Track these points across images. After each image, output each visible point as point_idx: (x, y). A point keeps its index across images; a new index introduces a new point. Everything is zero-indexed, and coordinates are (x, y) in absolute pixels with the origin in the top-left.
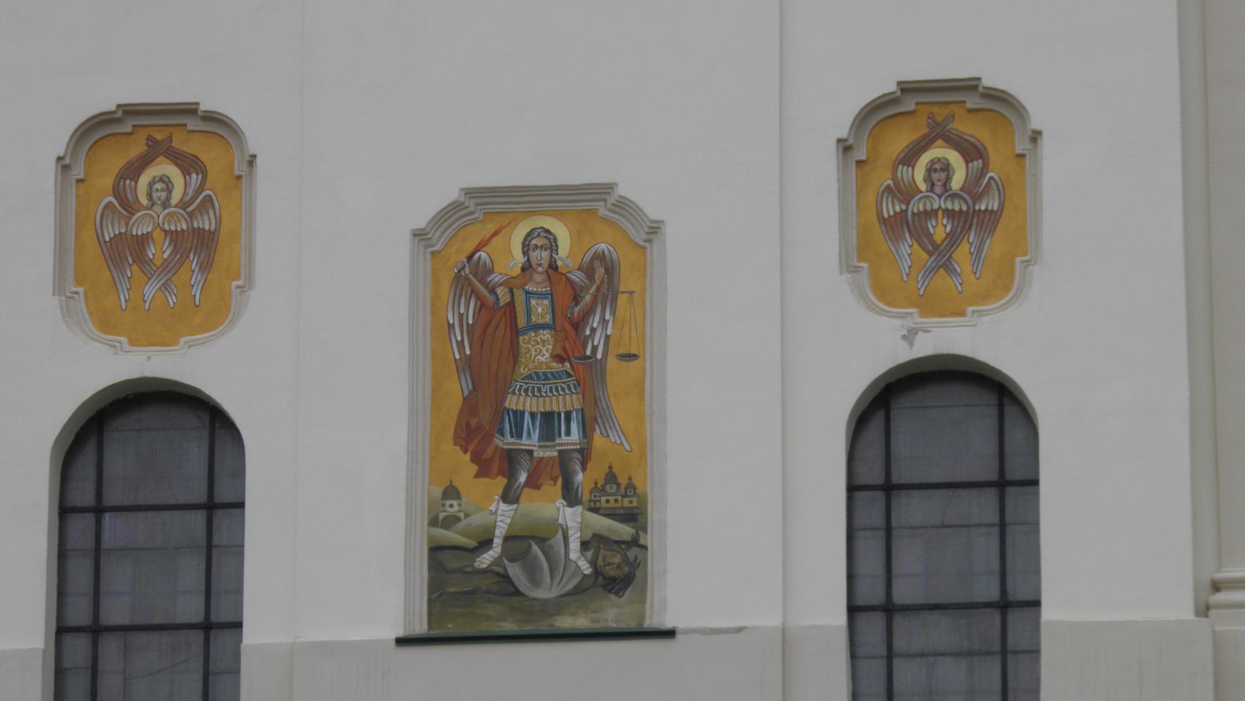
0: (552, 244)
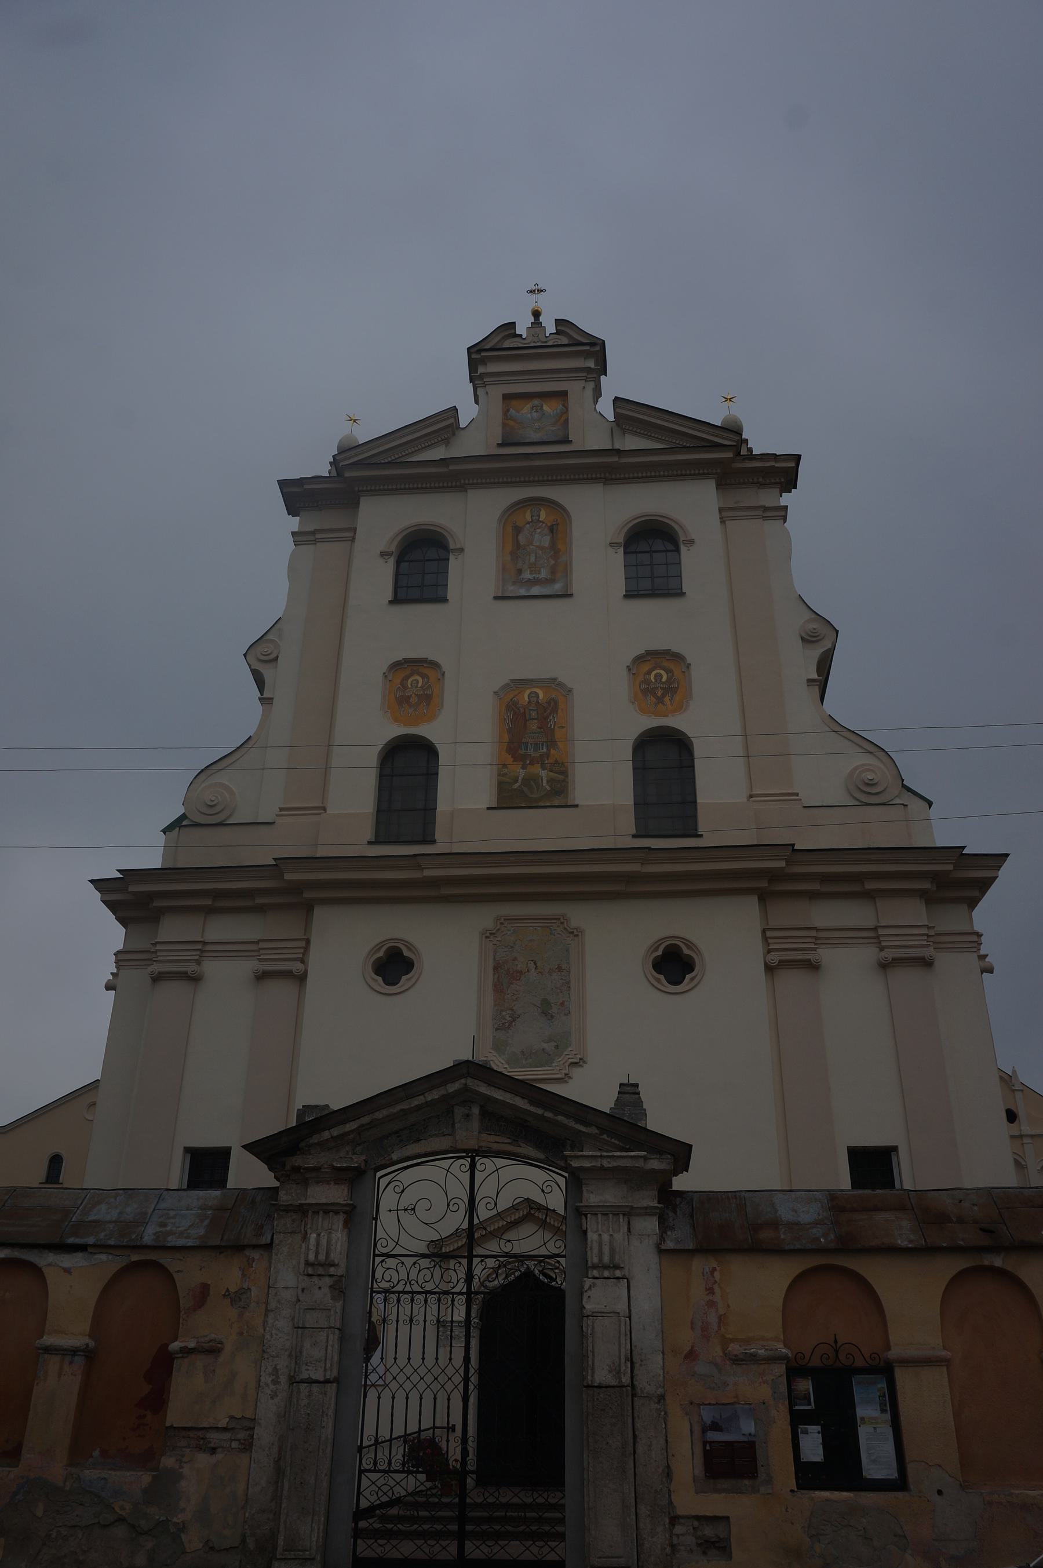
0: (537, 695)
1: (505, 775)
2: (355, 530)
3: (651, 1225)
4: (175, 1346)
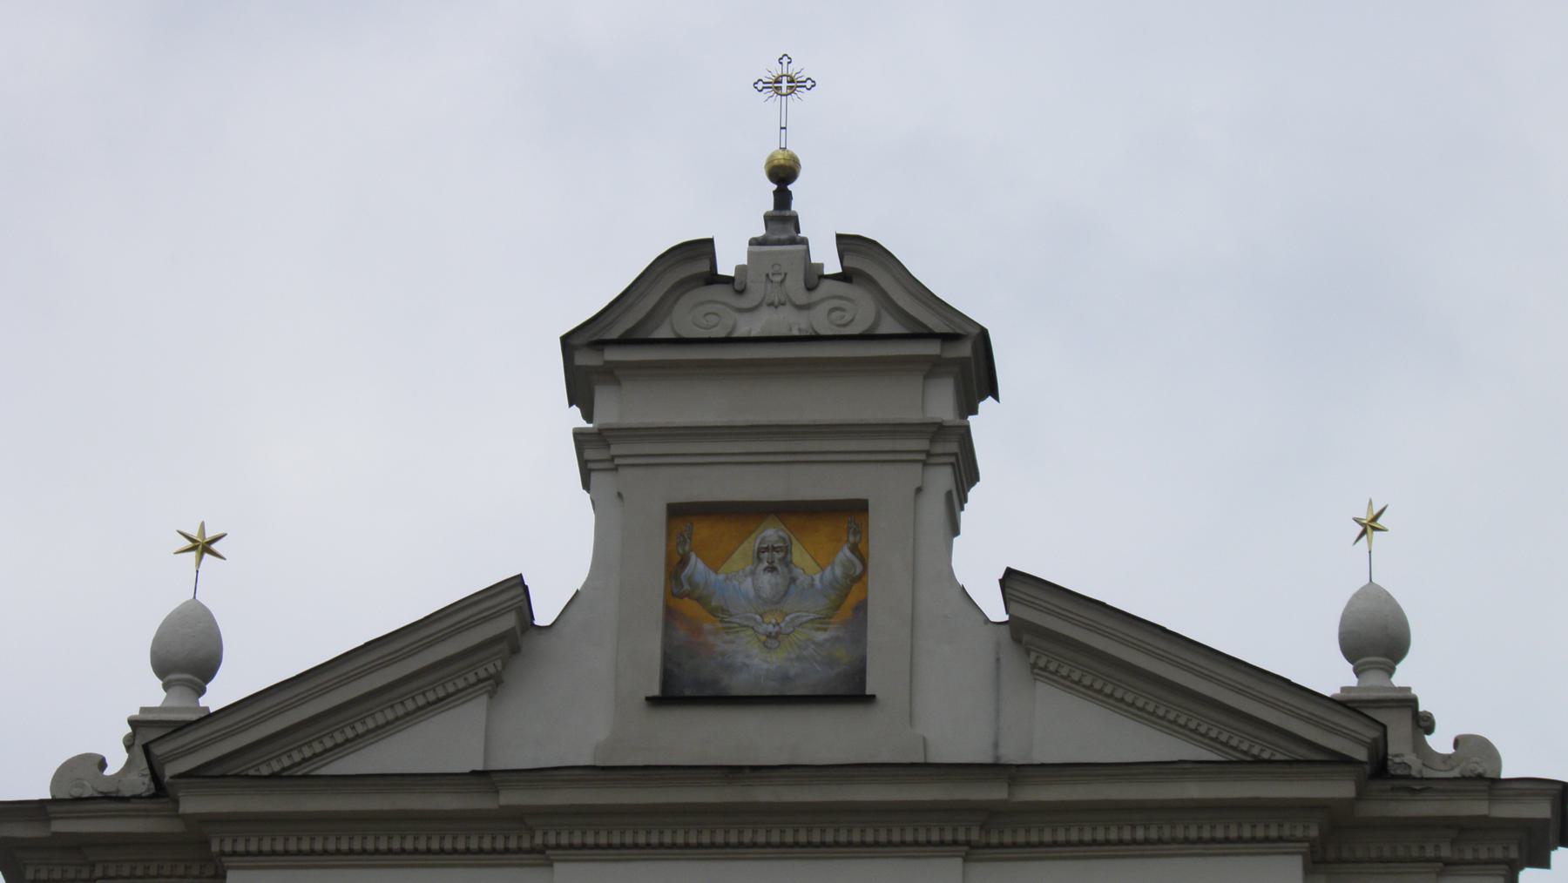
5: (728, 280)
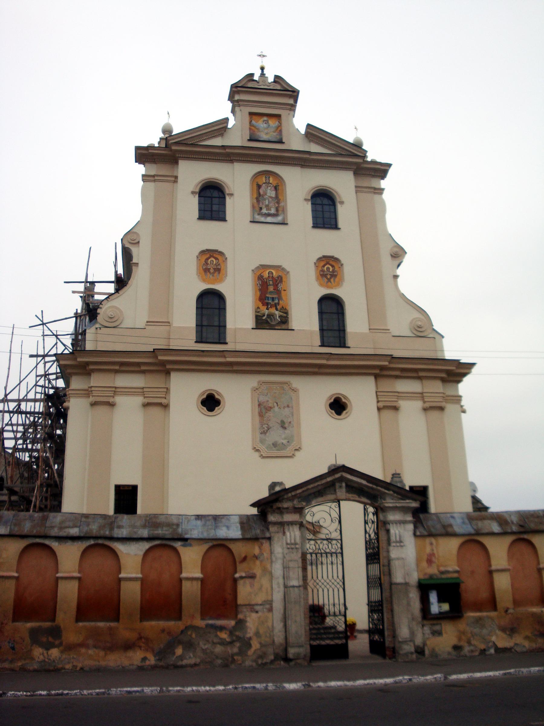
0: (272, 273)
1: (258, 312)
2: (176, 177)
3: (411, 527)
4: (237, 575)
5: (256, 81)
